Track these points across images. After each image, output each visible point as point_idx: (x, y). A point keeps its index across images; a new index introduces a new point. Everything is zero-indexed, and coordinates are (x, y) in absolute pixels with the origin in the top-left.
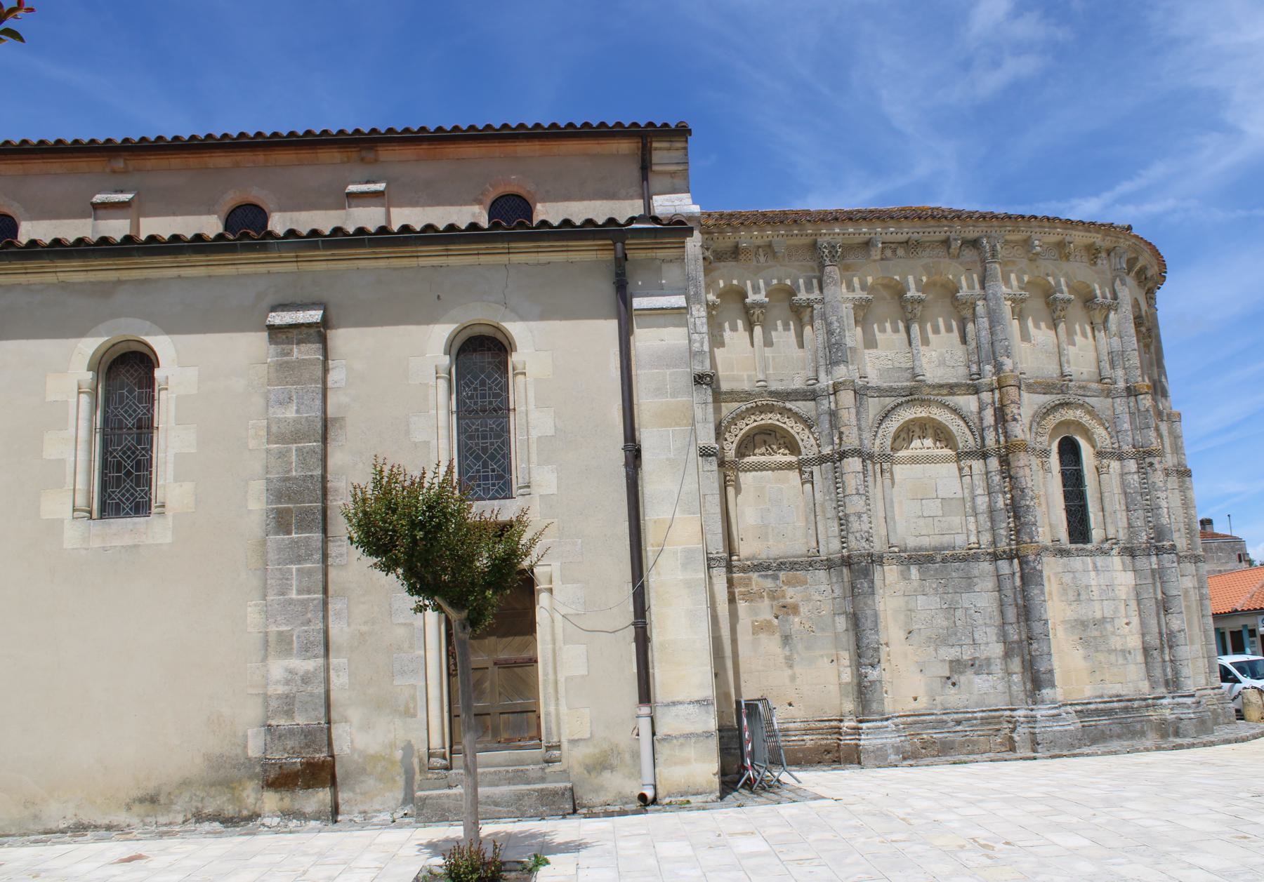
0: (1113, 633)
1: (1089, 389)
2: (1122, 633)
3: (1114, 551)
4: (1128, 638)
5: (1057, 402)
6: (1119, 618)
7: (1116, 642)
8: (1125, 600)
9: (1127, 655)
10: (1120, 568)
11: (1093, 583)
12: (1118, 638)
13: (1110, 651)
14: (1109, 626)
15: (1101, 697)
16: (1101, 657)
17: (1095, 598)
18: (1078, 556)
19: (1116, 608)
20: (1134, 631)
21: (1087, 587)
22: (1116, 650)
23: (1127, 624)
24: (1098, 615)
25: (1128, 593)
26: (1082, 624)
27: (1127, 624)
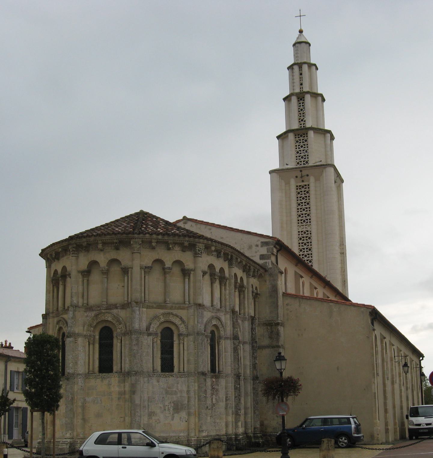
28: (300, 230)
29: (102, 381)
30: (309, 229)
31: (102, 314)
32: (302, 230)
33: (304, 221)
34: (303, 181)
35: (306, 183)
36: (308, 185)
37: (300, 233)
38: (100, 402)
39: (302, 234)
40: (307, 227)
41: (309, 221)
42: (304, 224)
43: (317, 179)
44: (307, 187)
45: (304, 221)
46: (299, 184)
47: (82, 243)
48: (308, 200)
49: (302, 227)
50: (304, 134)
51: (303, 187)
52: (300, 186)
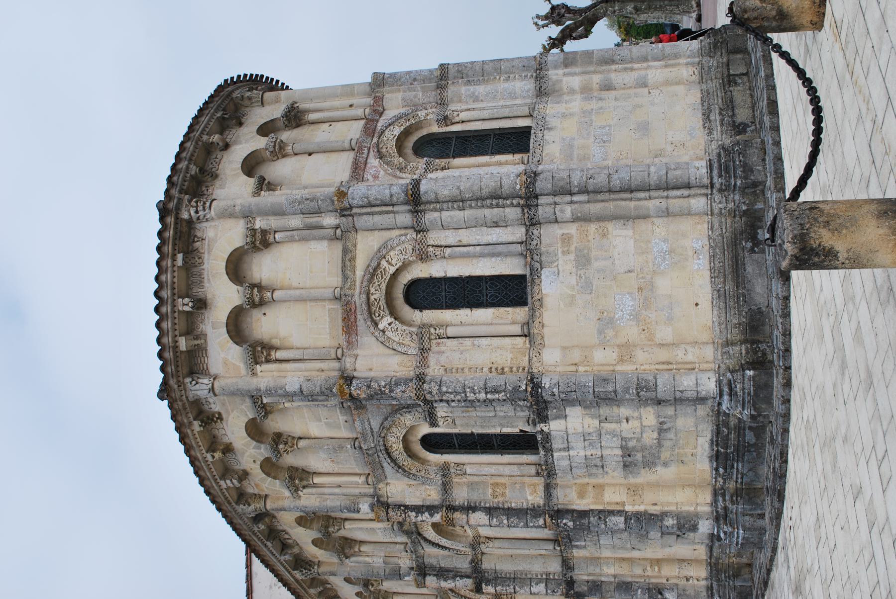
0: (638, 440)
1: (364, 429)
2: (638, 430)
4: (644, 424)
6: (621, 431)
7: (650, 437)
8: (600, 422)
9: (665, 427)
10: (563, 422)
12: (644, 435)
13: (660, 445)
14: (631, 444)
16: (665, 455)
17: (599, 453)
19: (607, 433)
20: (636, 414)
22: (658, 439)
23: (627, 420)
24: (619, 452)
25: (593, 417)
27: (627, 420)
29: (549, 129)
31: (381, 146)
38: (607, 128)
47: (188, 175)
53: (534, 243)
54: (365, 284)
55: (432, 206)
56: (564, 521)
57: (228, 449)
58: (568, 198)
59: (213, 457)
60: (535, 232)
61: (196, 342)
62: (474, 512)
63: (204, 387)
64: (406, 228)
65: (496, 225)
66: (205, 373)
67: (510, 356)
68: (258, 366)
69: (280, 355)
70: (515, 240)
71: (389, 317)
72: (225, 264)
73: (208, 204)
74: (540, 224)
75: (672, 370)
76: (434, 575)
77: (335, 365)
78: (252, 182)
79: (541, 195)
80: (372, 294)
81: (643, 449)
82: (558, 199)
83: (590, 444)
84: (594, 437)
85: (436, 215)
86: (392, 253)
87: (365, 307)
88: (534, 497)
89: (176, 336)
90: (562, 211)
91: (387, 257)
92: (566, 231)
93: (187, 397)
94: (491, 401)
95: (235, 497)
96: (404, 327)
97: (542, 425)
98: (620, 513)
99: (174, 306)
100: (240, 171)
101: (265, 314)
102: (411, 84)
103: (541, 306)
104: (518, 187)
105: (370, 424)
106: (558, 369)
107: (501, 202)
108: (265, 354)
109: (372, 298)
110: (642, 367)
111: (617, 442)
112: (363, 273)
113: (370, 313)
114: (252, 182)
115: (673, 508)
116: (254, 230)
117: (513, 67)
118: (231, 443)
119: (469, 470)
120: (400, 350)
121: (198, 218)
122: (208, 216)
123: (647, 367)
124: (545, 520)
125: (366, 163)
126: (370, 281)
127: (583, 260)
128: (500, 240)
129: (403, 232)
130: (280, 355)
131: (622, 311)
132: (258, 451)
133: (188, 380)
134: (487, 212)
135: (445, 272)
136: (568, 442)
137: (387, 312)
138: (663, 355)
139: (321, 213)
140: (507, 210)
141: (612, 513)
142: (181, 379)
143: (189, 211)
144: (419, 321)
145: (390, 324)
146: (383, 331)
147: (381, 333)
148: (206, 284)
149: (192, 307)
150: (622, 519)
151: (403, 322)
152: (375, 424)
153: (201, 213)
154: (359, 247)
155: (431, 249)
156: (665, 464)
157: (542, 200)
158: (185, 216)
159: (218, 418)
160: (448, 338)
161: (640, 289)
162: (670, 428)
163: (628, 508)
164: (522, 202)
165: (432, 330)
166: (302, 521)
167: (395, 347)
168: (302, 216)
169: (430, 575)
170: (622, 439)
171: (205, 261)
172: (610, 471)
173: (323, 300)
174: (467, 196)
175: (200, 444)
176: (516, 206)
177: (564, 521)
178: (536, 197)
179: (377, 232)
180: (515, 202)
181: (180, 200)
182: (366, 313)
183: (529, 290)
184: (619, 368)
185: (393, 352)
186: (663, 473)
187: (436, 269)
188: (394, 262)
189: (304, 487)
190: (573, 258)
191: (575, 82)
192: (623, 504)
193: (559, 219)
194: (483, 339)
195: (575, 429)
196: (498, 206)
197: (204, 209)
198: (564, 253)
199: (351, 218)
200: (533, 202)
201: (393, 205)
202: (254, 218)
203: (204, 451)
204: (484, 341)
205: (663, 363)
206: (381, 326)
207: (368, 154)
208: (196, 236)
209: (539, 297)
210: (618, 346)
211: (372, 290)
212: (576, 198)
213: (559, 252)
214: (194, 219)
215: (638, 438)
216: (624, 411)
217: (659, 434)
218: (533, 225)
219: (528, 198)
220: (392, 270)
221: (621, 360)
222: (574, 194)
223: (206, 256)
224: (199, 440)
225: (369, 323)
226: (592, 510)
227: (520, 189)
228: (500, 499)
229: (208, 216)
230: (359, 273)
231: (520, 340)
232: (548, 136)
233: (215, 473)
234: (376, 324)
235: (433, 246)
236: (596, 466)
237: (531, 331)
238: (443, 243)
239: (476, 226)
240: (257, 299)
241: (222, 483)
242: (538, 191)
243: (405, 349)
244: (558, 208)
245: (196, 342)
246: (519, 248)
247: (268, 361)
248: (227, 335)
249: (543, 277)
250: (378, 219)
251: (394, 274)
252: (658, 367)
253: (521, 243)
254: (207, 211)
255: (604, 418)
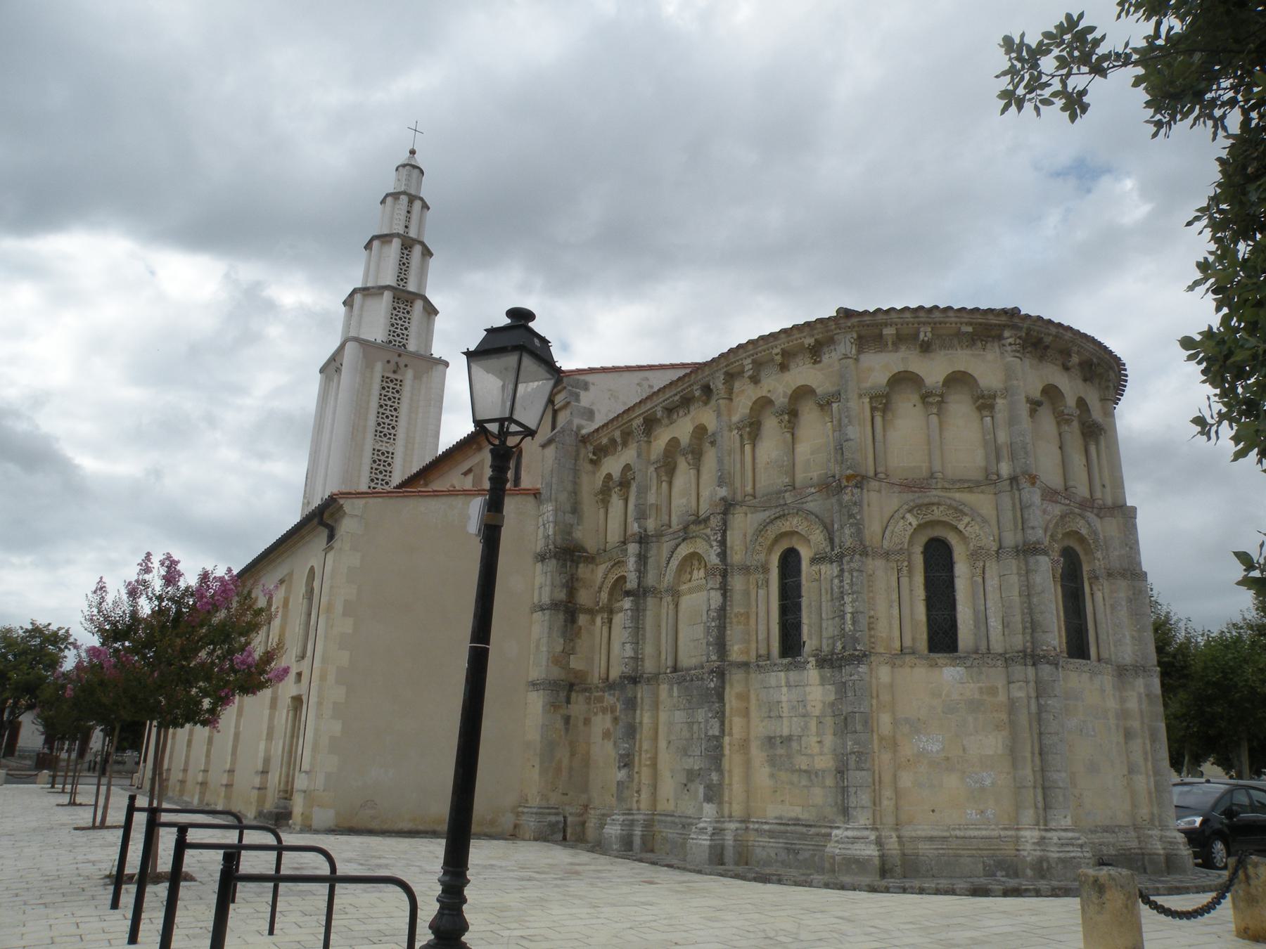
2: (809, 752)
3: (810, 665)
5: (773, 517)
7: (802, 762)
8: (817, 717)
11: (784, 698)
12: (803, 757)
13: (794, 771)
14: (795, 745)
15: (780, 818)
16: (783, 776)
17: (784, 715)
18: (773, 671)
20: (826, 750)
21: (779, 702)
23: (819, 742)
24: (786, 732)
26: (770, 741)
27: (819, 742)
28: (377, 447)
29: (1091, 678)
30: (391, 450)
32: (380, 448)
33: (385, 435)
34: (395, 372)
35: (399, 378)
36: (401, 381)
37: (376, 452)
39: (378, 455)
40: (388, 445)
41: (392, 437)
42: (385, 439)
43: (417, 377)
44: (398, 383)
45: (385, 435)
46: (387, 375)
48: (396, 404)
49: (381, 443)
50: (407, 302)
51: (392, 381)
52: (388, 378)
53: (989, 661)
54: (949, 502)
55: (1024, 567)
56: (715, 679)
57: (784, 367)
58: (1033, 694)
59: (777, 355)
60: (1000, 662)
61: (890, 343)
62: (722, 594)
63: (848, 351)
64: (1000, 540)
65: (1005, 625)
66: (860, 350)
67: (884, 635)
68: (868, 400)
69: (878, 420)
70: (991, 643)
71: (917, 523)
72: (963, 369)
73: (1018, 355)
74: (1007, 667)
75: (874, 784)
76: (640, 552)
77: (871, 473)
78: (1037, 395)
79: (1036, 669)
80: (938, 508)
81: (789, 756)
82: (1032, 684)
83: (793, 707)
84: (801, 710)
85: (1015, 570)
86: (977, 527)
87: (926, 500)
88: (736, 652)
89: (896, 325)
90: (1020, 688)
91: (973, 523)
92: (1000, 691)
93: (838, 334)
94: (842, 617)
95: (730, 371)
96: (908, 537)
97: (814, 662)
98: (722, 731)
99: (924, 324)
100: (1046, 383)
101: (915, 406)
102: (1126, 545)
103: (931, 666)
104: (1045, 648)
105: (812, 501)
106: (874, 680)
107: (1029, 631)
108: (880, 406)
109: (935, 508)
110: (876, 758)
111: (796, 731)
112: (957, 499)
113: (919, 507)
114: (1037, 395)
115: (727, 781)
116: (995, 399)
117: (1146, 644)
118: (789, 370)
119: (762, 592)
120: (887, 532)
121: (1004, 345)
122: (1006, 355)
123: (877, 762)
124: (714, 661)
125: (1057, 502)
126: (950, 507)
127: (974, 706)
128: (991, 630)
129: (997, 538)
130: (878, 420)
131: (927, 741)
132: (782, 395)
133: (855, 335)
134: (1018, 618)
135: (959, 577)
136: (796, 686)
137: (922, 521)
138: (887, 778)
139: (1013, 461)
140: (1020, 637)
141: (722, 723)
142: (856, 329)
143: (1011, 337)
144: (913, 551)
145: (910, 524)
146: (903, 518)
147: (901, 516)
148: (943, 352)
149: (923, 340)
150: (717, 734)
151: (912, 536)
152: (811, 506)
153: (1009, 348)
154: (981, 496)
155: (981, 564)
156: (772, 776)
157: (1031, 671)
158: (1007, 334)
159: (815, 360)
160: (898, 579)
161: (948, 759)
162: (811, 780)
163: (727, 739)
164: (1029, 650)
165: (906, 564)
166: (700, 431)
167: (889, 528)
168: (1009, 443)
169: (640, 547)
170: (800, 737)
171: (965, 351)
172: (764, 724)
173: (930, 462)
174: (1035, 600)
175: (791, 343)
176: (1024, 645)
177: (715, 679)
178: (1034, 664)
179: (996, 512)
180: (1028, 644)
181: (1020, 329)
182: (920, 501)
183: (945, 655)
184: (875, 737)
185: (885, 525)
186: (762, 775)
187: (962, 570)
188: (968, 529)
189: (741, 436)
190: (975, 697)
191: (1132, 704)
192: (731, 734)
193: (1012, 686)
194: (898, 611)
195: (810, 693)
196: (1024, 628)
197: (1015, 351)
198: (981, 688)
199: (1009, 489)
200: (1029, 661)
201: (1023, 529)
202: (1005, 398)
203: (783, 346)
204: (896, 612)
205: (880, 778)
206: (908, 516)
207: (1063, 504)
208: (987, 343)
209: (939, 664)
210: (894, 737)
211: (941, 508)
212: (1033, 701)
213: (981, 685)
214: (1003, 342)
215: (800, 751)
216: (829, 740)
217: (805, 771)
218: (1006, 660)
219: (1033, 656)
220: (961, 527)
221: (881, 739)
222: (1038, 700)
223: (969, 352)
224: (791, 343)
225: (912, 504)
226: (724, 705)
227: (1043, 650)
228: (735, 620)
229: (1006, 355)
230: (957, 496)
231: (897, 645)
232: (1085, 676)
233: (759, 355)
234: (910, 511)
235: (984, 566)
236: (770, 711)
237: (907, 656)
238: (987, 576)
239: (1003, 606)
240: (931, 400)
241: (749, 361)
242: (1040, 666)
243: (888, 538)
244: (1024, 684)
245: (890, 343)
246: (983, 648)
247: (873, 409)
248: (897, 371)
249: (958, 669)
250: (1009, 515)
251: (957, 528)
252: (877, 772)
253: (988, 649)
254: (1012, 354)
255: (822, 720)
